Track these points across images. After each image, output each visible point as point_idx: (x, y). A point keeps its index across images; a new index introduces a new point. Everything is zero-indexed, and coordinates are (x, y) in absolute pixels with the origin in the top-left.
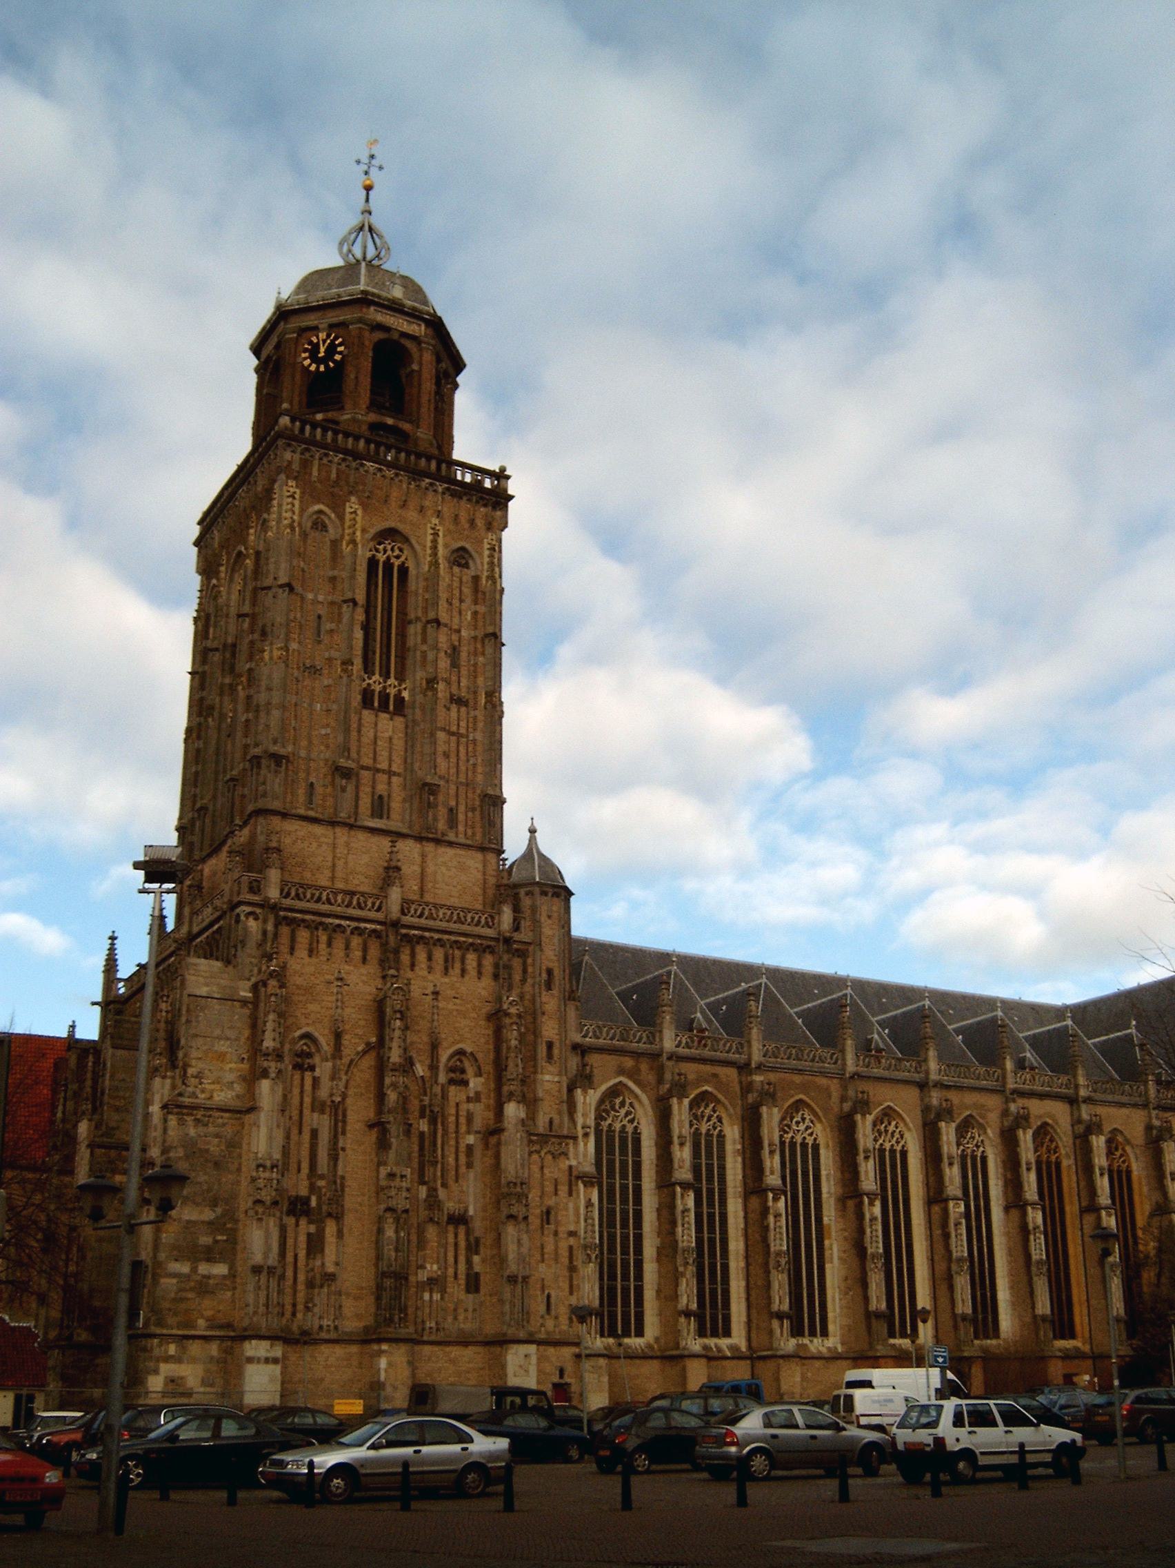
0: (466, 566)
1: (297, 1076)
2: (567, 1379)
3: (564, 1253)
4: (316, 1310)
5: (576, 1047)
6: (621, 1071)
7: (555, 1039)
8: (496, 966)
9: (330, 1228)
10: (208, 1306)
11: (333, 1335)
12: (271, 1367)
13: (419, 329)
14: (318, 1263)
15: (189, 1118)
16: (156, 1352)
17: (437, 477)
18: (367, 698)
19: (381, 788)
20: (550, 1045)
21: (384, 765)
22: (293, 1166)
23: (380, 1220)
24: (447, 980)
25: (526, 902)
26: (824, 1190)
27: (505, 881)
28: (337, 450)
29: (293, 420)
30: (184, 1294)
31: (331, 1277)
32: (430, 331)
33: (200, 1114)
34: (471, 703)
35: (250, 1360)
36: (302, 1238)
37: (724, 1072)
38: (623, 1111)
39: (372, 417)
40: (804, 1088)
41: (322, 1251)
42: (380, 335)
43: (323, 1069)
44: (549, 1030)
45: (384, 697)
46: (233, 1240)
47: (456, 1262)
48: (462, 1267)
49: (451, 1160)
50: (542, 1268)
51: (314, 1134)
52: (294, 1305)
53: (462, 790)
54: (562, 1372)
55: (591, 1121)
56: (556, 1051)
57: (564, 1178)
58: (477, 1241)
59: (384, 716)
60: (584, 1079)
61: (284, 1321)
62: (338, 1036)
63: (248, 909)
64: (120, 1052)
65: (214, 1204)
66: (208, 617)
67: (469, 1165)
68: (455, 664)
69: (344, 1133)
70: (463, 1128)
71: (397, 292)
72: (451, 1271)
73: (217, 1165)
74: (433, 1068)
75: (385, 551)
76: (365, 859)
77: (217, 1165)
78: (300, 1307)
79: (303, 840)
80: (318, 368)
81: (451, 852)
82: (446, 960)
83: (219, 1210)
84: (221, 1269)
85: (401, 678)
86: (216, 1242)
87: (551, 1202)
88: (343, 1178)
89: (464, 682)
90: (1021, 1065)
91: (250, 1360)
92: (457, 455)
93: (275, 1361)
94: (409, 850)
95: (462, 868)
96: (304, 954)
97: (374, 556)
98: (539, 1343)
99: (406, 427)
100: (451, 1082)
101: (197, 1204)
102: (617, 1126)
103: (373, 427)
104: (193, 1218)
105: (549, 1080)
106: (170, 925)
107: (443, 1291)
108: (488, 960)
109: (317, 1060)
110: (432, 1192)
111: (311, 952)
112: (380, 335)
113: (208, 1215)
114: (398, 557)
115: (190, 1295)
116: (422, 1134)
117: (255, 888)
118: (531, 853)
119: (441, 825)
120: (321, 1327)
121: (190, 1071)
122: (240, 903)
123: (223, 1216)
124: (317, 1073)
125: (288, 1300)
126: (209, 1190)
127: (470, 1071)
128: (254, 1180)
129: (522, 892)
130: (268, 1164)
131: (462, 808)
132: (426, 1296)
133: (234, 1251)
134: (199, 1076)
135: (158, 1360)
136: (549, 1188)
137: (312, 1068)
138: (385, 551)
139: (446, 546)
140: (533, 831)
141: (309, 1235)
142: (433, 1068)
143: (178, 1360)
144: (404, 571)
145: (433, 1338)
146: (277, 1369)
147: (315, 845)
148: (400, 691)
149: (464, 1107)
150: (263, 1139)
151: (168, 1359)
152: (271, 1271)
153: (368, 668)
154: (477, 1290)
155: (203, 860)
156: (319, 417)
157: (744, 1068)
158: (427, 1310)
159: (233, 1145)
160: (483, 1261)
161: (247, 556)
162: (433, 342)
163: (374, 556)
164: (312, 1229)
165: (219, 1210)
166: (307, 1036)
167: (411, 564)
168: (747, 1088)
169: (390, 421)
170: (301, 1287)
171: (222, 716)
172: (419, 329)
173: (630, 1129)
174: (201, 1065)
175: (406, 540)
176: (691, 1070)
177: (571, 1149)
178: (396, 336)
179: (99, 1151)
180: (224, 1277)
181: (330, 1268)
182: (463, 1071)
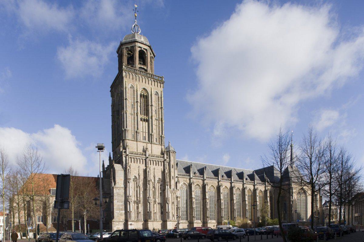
6: (184, 181)
20: (173, 177)
27: (165, 150)
29: (125, 67)
32: (149, 48)
39: (140, 66)
42: (140, 49)
44: (172, 174)
49: (158, 195)
59: (144, 123)
64: (106, 179)
66: (113, 105)
68: (156, 113)
75: (143, 92)
90: (246, 179)
94: (149, 145)
97: (141, 93)
99: (146, 68)
103: (140, 68)
105: (173, 182)
106: (112, 159)
114: (145, 93)
117: (125, 152)
119: (155, 141)
131: (158, 138)
135: (115, 225)
139: (153, 91)
148: (147, 118)
154: (163, 214)
155: (116, 148)
160: (163, 210)
161: (119, 94)
163: (141, 93)
169: (142, 67)
171: (117, 123)
176: (195, 180)
177: (177, 193)
178: (142, 49)
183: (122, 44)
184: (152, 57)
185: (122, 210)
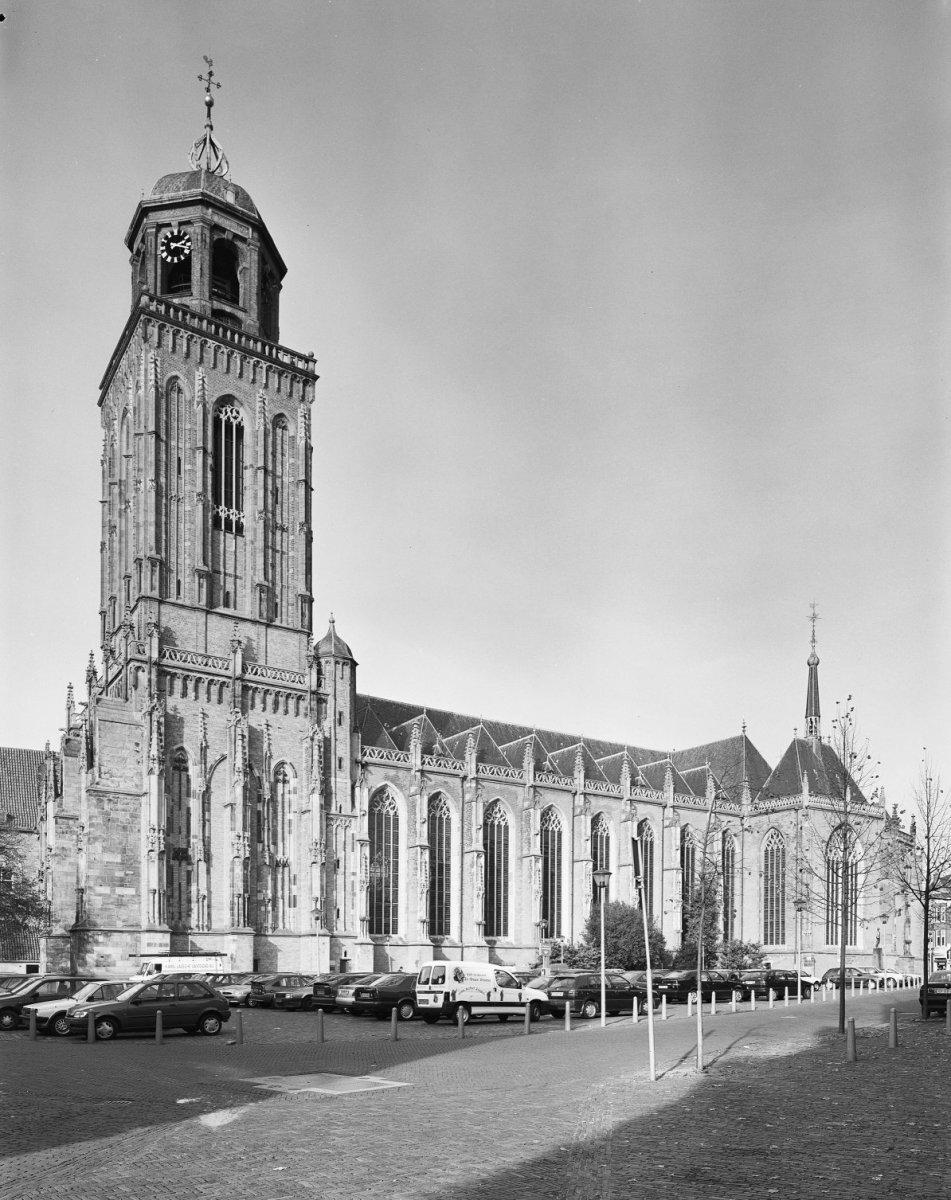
6: (387, 778)
10: (123, 913)
13: (248, 233)
15: (105, 799)
18: (217, 519)
22: (176, 830)
24: (274, 716)
28: (187, 327)
30: (108, 907)
32: (256, 235)
34: (290, 529)
38: (387, 803)
45: (228, 522)
46: (137, 874)
71: (230, 198)
73: (124, 828)
75: (226, 413)
77: (124, 828)
80: (172, 260)
85: (239, 508)
86: (127, 875)
92: (281, 342)
101: (113, 852)
102: (384, 811)
114: (235, 418)
115: (111, 906)
126: (120, 843)
138: (226, 413)
144: (240, 429)
147: (183, 623)
156: (176, 301)
162: (259, 244)
169: (228, 309)
180: (133, 896)
183: (144, 211)
184: (271, 274)
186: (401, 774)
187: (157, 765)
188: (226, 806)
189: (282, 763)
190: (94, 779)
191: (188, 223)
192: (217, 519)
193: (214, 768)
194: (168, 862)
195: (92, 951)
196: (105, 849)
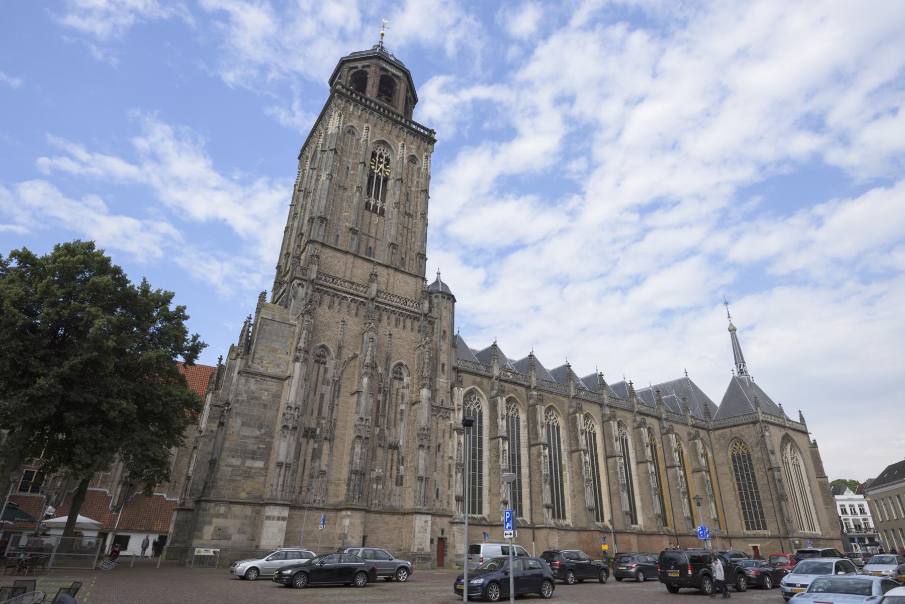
0: (415, 163)
1: (316, 366)
2: (445, 536)
3: (447, 467)
4: (313, 491)
5: (454, 369)
6: (474, 383)
7: (446, 362)
8: (420, 327)
9: (326, 446)
10: (249, 485)
11: (322, 505)
12: (281, 522)
13: (400, 74)
14: (317, 464)
16: (212, 511)
17: (404, 125)
18: (367, 205)
19: (371, 244)
20: (443, 365)
21: (373, 235)
22: (309, 412)
23: (354, 442)
25: (435, 301)
26: (562, 448)
31: (323, 473)
33: (259, 378)
35: (268, 518)
36: (310, 451)
37: (519, 388)
40: (553, 400)
41: (320, 458)
42: (383, 73)
43: (331, 364)
44: (443, 358)
45: (375, 207)
46: (269, 448)
47: (391, 469)
48: (394, 472)
49: (392, 416)
50: (435, 474)
51: (322, 396)
52: (301, 488)
53: (408, 251)
54: (443, 531)
55: (461, 402)
56: (446, 368)
57: (448, 430)
58: (403, 458)
59: (374, 215)
60: (459, 383)
61: (294, 496)
62: (340, 348)
63: (299, 282)
65: (260, 427)
67: (401, 420)
69: (338, 397)
70: (400, 401)
72: (388, 474)
73: (265, 406)
74: (387, 369)
76: (360, 271)
78: (304, 489)
79: (331, 257)
81: (401, 275)
82: (396, 320)
83: (263, 431)
84: (259, 464)
86: (259, 448)
87: (440, 441)
88: (335, 420)
89: (412, 208)
91: (268, 518)
93: (284, 519)
95: (407, 284)
96: (326, 308)
98: (433, 515)
100: (395, 378)
101: (250, 426)
102: (472, 408)
104: (247, 434)
107: (384, 484)
108: (417, 324)
109: (327, 359)
110: (382, 430)
111: (330, 307)
112: (383, 73)
113: (257, 433)
116: (379, 401)
118: (437, 283)
120: (314, 501)
121: (256, 356)
122: (295, 278)
123: (265, 434)
124: (327, 366)
125: (298, 484)
126: (258, 419)
127: (405, 373)
128: (284, 414)
129: (433, 296)
130: (293, 406)
131: (408, 259)
132: (375, 486)
133: (269, 455)
134: (261, 359)
135: (213, 516)
136: (440, 434)
137: (325, 363)
140: (439, 274)
141: (314, 449)
142: (387, 369)
143: (225, 516)
145: (376, 509)
146: (285, 523)
149: (401, 390)
150: (292, 394)
151: (219, 516)
152: (288, 466)
153: (369, 193)
154: (401, 485)
157: (528, 388)
158: (374, 494)
159: (277, 397)
160: (406, 469)
164: (316, 446)
165: (263, 431)
166: (323, 347)
167: (390, 157)
168: (529, 398)
170: (306, 477)
172: (400, 74)
173: (478, 410)
174: (263, 353)
175: (389, 147)
179: (214, 408)
180: (261, 469)
181: (324, 468)
182: (401, 374)
185: (253, 458)
186: (485, 381)
187: (302, 355)
188: (353, 394)
189: (400, 364)
190: (247, 363)
191: (368, 66)
192: (367, 205)
193: (346, 363)
194: (298, 439)
195: (210, 523)
196: (243, 424)
